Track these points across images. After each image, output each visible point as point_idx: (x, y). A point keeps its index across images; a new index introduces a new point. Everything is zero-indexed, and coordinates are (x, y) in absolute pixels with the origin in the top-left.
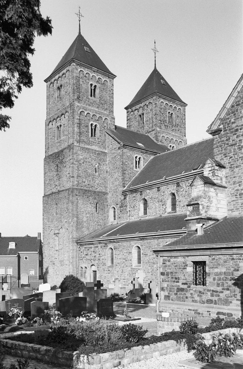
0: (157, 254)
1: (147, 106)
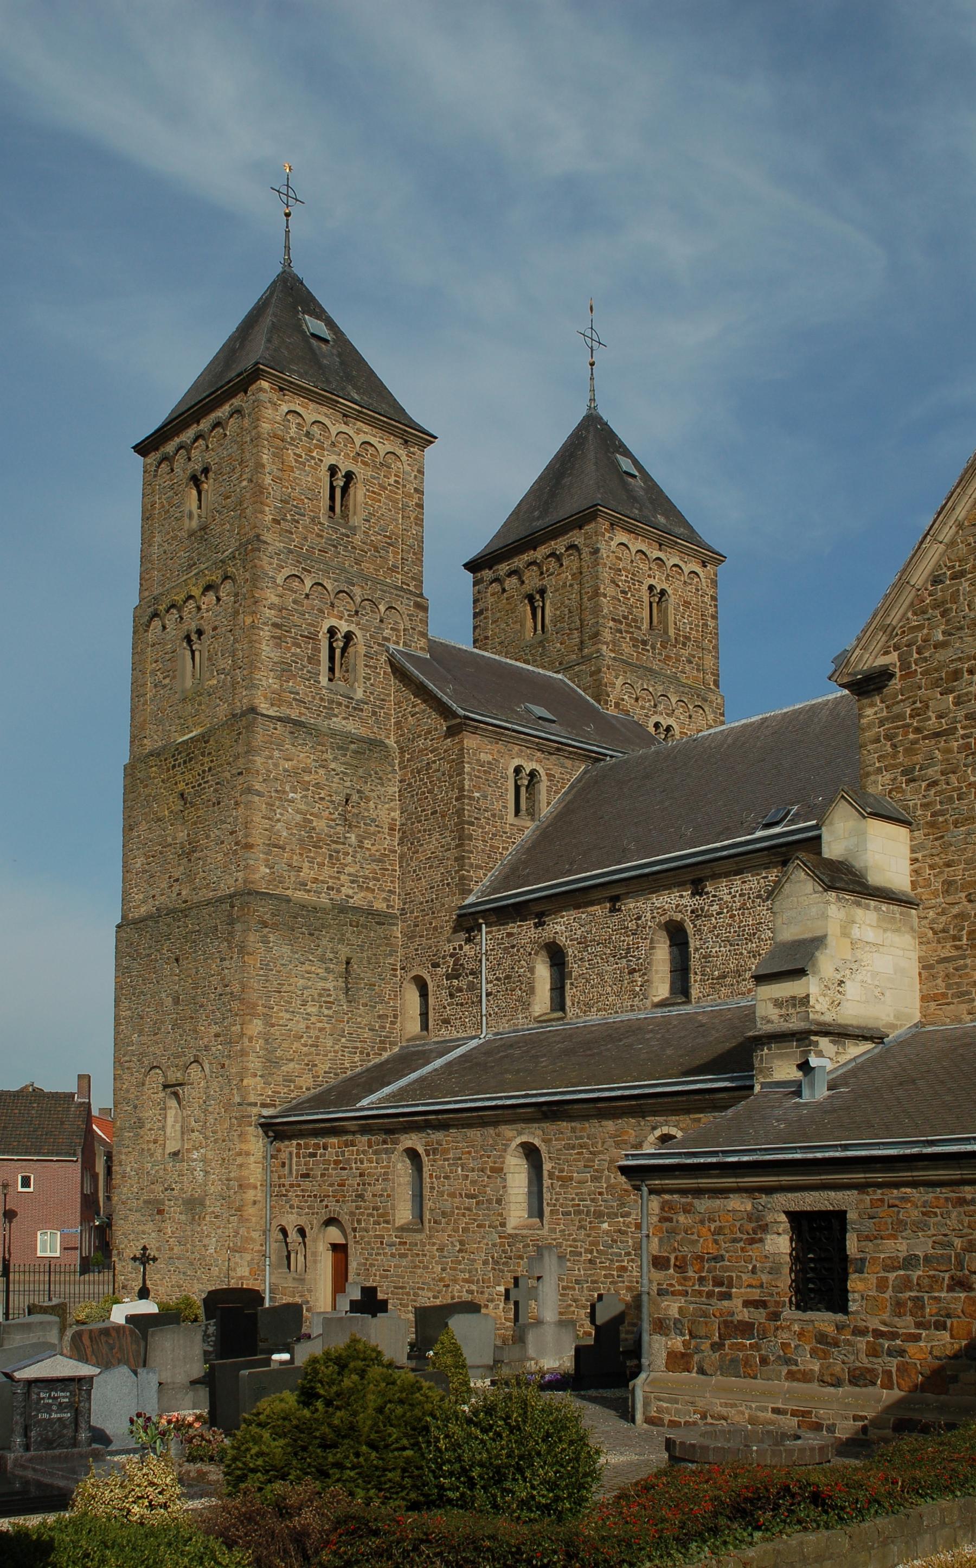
0: (638, 1183)
1: (558, 558)
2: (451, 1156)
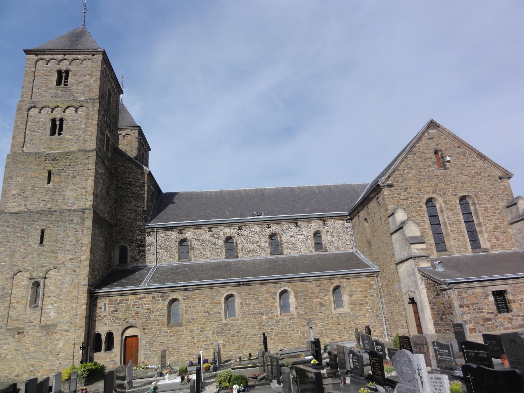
2: (196, 300)
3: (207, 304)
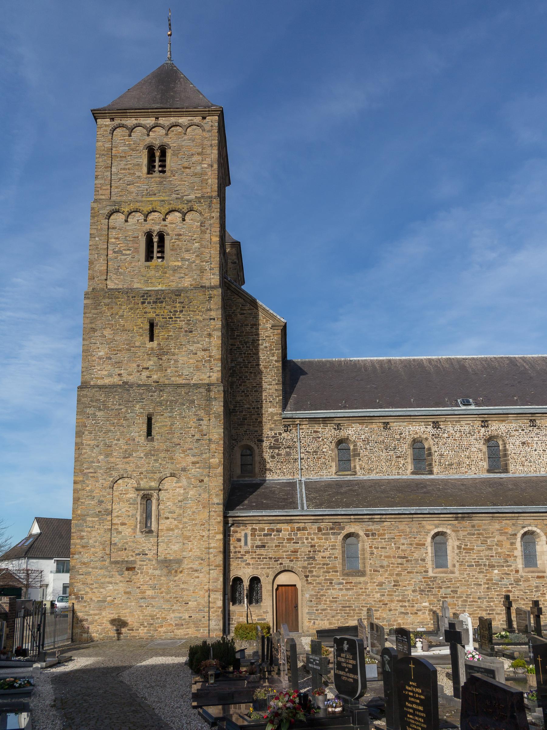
2: (386, 537)
3: (403, 544)
